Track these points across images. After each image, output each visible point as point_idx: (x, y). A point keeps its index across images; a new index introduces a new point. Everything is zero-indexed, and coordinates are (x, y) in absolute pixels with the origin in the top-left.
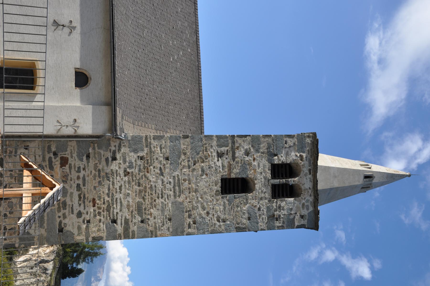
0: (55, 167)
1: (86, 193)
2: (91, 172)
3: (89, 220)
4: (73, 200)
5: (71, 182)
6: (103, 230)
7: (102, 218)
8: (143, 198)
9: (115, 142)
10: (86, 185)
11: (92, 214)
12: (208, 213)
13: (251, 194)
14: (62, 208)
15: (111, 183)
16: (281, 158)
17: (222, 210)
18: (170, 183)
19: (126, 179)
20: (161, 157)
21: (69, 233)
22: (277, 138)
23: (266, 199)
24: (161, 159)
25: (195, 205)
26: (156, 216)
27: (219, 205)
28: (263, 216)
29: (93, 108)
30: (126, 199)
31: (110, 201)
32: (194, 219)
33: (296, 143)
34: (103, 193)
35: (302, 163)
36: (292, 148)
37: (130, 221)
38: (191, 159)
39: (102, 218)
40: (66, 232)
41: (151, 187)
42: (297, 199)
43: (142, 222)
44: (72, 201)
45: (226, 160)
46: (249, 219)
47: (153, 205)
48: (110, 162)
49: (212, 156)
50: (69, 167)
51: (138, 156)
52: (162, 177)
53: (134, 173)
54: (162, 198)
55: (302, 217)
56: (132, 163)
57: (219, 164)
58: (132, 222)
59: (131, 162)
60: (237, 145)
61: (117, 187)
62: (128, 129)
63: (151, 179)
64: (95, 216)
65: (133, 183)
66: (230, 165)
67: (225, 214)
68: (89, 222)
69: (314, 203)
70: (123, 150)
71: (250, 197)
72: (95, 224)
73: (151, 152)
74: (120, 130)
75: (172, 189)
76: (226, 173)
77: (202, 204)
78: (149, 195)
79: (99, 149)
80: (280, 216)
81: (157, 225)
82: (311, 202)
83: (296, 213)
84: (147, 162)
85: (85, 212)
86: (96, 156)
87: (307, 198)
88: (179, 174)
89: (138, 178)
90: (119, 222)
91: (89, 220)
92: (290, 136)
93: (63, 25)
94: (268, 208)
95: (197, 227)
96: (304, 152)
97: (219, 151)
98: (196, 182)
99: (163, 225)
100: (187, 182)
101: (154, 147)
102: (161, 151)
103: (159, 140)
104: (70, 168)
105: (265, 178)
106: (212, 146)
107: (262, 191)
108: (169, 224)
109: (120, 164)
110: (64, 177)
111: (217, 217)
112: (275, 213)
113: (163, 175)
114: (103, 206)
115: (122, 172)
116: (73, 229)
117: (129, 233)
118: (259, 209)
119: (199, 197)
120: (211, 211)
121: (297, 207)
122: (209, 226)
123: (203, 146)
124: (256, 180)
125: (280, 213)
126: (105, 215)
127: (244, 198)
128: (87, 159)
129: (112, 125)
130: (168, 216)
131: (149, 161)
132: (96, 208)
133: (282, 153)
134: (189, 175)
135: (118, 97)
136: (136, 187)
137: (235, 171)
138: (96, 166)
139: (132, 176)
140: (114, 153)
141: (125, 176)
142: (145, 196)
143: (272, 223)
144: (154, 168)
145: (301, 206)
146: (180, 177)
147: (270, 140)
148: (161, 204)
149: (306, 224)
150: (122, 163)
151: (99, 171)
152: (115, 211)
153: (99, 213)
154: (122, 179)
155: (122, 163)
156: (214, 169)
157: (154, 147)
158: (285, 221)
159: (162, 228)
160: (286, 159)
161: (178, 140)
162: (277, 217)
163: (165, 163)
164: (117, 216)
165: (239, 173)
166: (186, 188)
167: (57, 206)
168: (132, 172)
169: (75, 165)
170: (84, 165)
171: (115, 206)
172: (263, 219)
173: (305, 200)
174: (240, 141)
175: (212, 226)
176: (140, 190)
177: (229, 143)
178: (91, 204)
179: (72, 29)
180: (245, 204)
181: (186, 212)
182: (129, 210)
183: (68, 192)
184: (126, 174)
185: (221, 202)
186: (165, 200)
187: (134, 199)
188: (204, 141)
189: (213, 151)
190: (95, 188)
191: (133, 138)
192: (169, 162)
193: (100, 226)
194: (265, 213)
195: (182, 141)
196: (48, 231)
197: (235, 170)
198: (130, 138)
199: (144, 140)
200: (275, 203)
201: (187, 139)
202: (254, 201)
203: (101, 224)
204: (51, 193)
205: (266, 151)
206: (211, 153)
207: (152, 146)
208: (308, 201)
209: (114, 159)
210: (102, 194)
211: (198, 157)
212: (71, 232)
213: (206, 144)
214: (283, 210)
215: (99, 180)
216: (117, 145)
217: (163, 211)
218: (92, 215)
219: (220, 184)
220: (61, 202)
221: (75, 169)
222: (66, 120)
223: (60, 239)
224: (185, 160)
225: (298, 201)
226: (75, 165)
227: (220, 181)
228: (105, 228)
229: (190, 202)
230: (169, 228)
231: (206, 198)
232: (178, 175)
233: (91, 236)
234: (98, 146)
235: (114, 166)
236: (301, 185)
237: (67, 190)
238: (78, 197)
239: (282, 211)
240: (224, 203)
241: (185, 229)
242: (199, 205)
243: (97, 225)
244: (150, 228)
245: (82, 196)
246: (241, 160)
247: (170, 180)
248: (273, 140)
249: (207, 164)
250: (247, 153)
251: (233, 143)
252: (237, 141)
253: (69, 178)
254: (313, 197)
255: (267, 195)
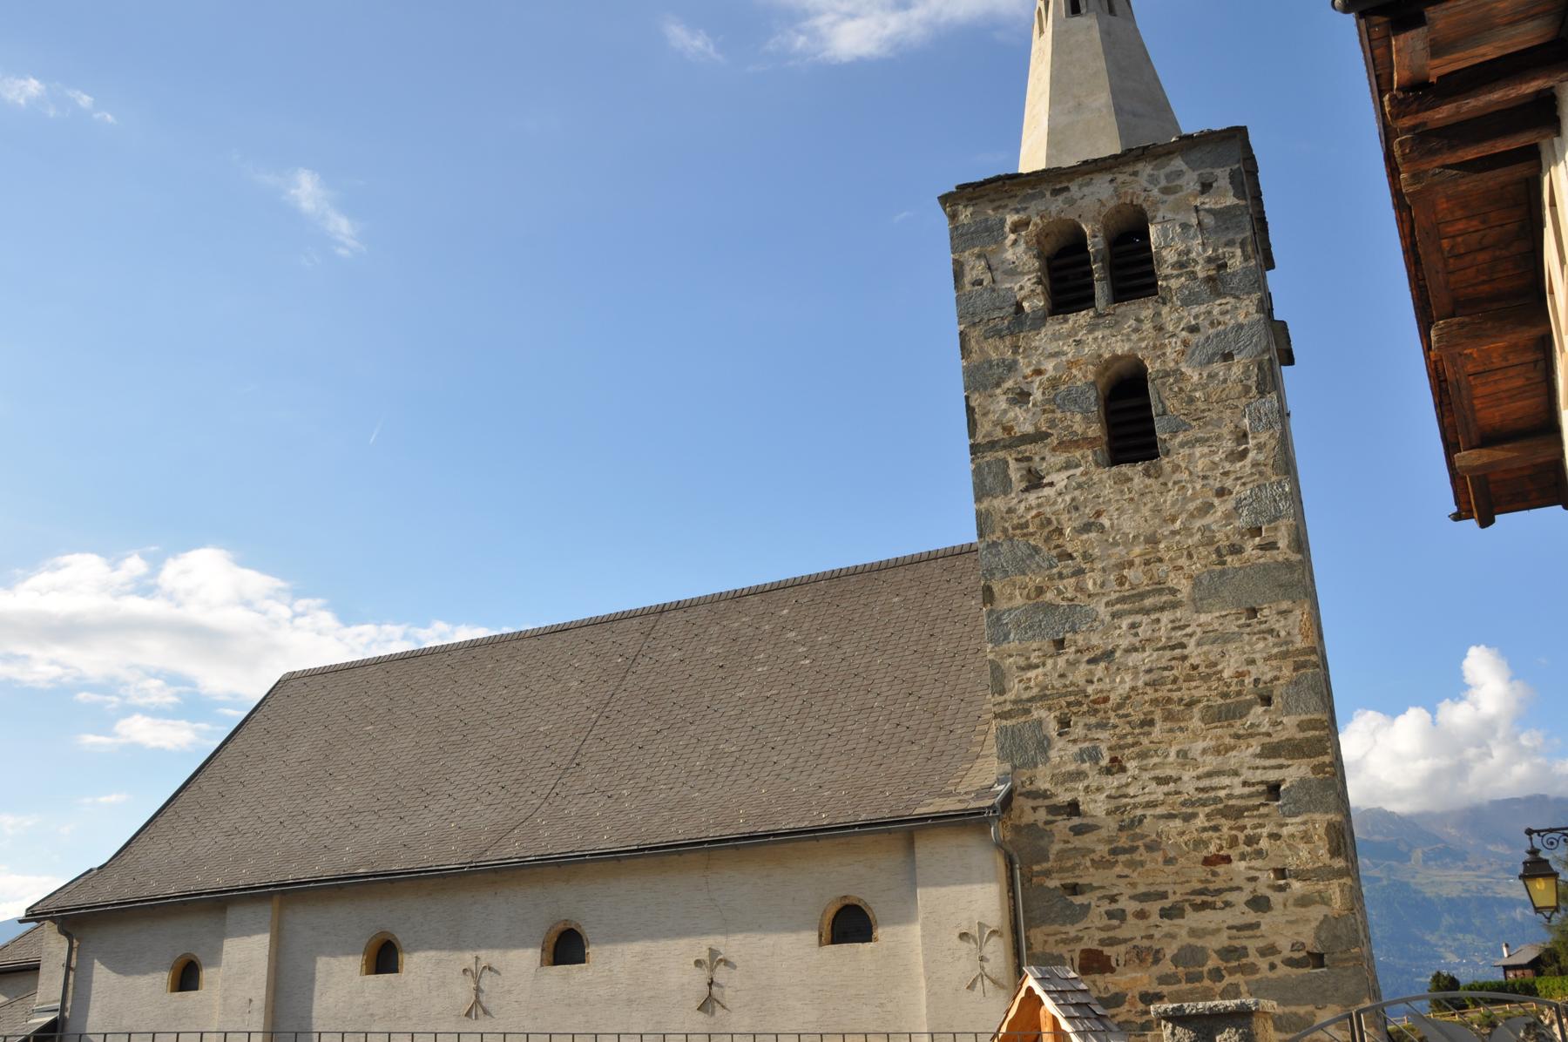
0: (1113, 989)
1: (1188, 888)
2: (1120, 876)
3: (1275, 870)
4: (1213, 926)
5: (1157, 935)
6: (1304, 823)
7: (1265, 831)
8: (1191, 704)
9: (1022, 811)
10: (1162, 889)
11: (1253, 863)
12: (1222, 492)
13: (1147, 363)
14: (1244, 961)
15: (1149, 812)
16: (1028, 289)
17: (1206, 450)
18: (1133, 626)
19: (1132, 765)
20: (1055, 664)
21: (1323, 936)
22: (967, 314)
23: (1158, 314)
24: (1061, 661)
25: (1198, 536)
26: (1246, 659)
27: (1191, 459)
28: (1216, 312)
29: (925, 885)
30: (1202, 761)
31: (1207, 810)
32: (1243, 535)
33: (976, 250)
34: (1182, 833)
35: (1036, 219)
36: (994, 262)
37: (1267, 740)
38: (1055, 571)
39: (1265, 831)
40: (1321, 942)
41: (1152, 684)
42: (1149, 215)
43: (1267, 701)
44: (1218, 930)
45: (1049, 460)
46: (1227, 357)
47: (1210, 672)
48: (1085, 821)
49: (1039, 506)
50: (1111, 945)
51: (1060, 735)
52: (1117, 654)
53: (1114, 741)
54: (1183, 646)
55: (1206, 187)
56: (1082, 751)
57: (1060, 479)
58: (1269, 735)
59: (1081, 756)
60: (999, 434)
61: (1159, 792)
62: (984, 776)
63: (1127, 686)
64: (1259, 854)
65: (1145, 741)
66: (1063, 445)
67: (1219, 438)
68: (1281, 873)
69: (1157, 157)
70: (1044, 784)
71: (1157, 365)
72: (1288, 852)
73: (1043, 697)
74: (982, 798)
75: (1153, 617)
76: (1089, 452)
77: (1192, 516)
78: (1180, 689)
79: (1047, 859)
80: (1209, 260)
81: (1275, 650)
82: (1156, 168)
83: (1197, 209)
84: (1075, 707)
85: (1249, 887)
86: (1069, 864)
87: (1145, 184)
88: (1105, 600)
89: (1128, 729)
90: (1273, 776)
91: (1275, 870)
92: (958, 275)
93: (710, 985)
94: (1187, 302)
95: (1270, 522)
96: (1003, 221)
97: (1023, 485)
98: (1125, 544)
99: (1271, 631)
100: (1125, 572)
101: (1026, 689)
102: (1037, 667)
103: (1003, 675)
104: (1112, 942)
105: (1092, 328)
106: (1010, 511)
107: (1136, 330)
108: (1266, 612)
109: (1087, 788)
110: (1142, 961)
111: (1232, 462)
112: (1201, 275)
113: (1113, 652)
114: (1225, 829)
115: (1113, 782)
116: (1308, 920)
117: (1307, 739)
118: (1193, 329)
119: (1172, 528)
120: (1211, 482)
121: (1177, 208)
122: (1262, 481)
123: (1011, 539)
124: (1100, 356)
125: (1201, 261)
126: (1256, 821)
127: (1164, 384)
128: (1082, 893)
129: (965, 824)
130: (1243, 621)
131: (1072, 698)
132: (1234, 854)
133: (1011, 289)
134: (1104, 570)
135: (885, 814)
136: (1157, 732)
137: (1078, 427)
138: (1100, 864)
139: (1121, 747)
140: (1054, 810)
141: (1123, 770)
142: (1181, 700)
143: (1236, 280)
144: (1090, 682)
145: (1172, 197)
146: (1114, 596)
147: (975, 333)
148: (1205, 648)
149: (1228, 169)
150: (1086, 783)
151: (1114, 852)
152: (1238, 791)
153: (1250, 841)
154: (1135, 778)
155: (1086, 783)
156: (1077, 493)
157: (1026, 689)
158: (1224, 240)
159: (1283, 634)
160: (1029, 272)
161: (999, 619)
162: (1213, 266)
163: (1073, 649)
164: (1253, 784)
165: (1085, 412)
166: (1145, 573)
167: (1238, 975)
168: (1110, 749)
169: (1101, 929)
170: (1099, 899)
171: (1222, 793)
172: (1224, 313)
173: (1150, 187)
174: (985, 427)
175: (1261, 474)
176: (1165, 719)
177: (997, 458)
178: (1221, 869)
179: (715, 959)
180: (1179, 375)
181: (1224, 563)
182: (1233, 748)
183: (1190, 946)
184: (1116, 766)
185: (1179, 457)
186: (1191, 635)
187: (1196, 736)
188: (997, 536)
189: (1022, 506)
190: (1169, 861)
191: (1004, 756)
192: (1068, 635)
193: (1292, 836)
194: (1203, 308)
195: (1002, 605)
196: (1321, 1000)
197: (1076, 427)
198: (1007, 767)
199: (1008, 723)
200: (1171, 280)
201: (995, 589)
202: (1169, 350)
203: (1285, 831)
204: (1049, 1006)
205: (1008, 340)
206: (1029, 509)
207: (1025, 696)
208: (1153, 180)
209: (1073, 808)
210: (1186, 838)
211: (1045, 549)
212: (1319, 928)
213: (1005, 530)
214: (1188, 252)
215: (1142, 849)
216: (1031, 803)
217: (1225, 639)
218: (1258, 863)
219: (1125, 468)
220: (1222, 965)
221: (1115, 928)
222: (963, 963)
223: (1346, 960)
224: (1058, 589)
225: (1158, 210)
226: (1101, 929)
227: (1114, 469)
228: (1298, 819)
229: (1190, 556)
230: (1280, 613)
231: (1173, 504)
232: (1107, 604)
233: (1328, 861)
234: (1038, 862)
235: (1096, 808)
236: (1104, 211)
237: (1181, 949)
238: (1203, 913)
239: (1193, 255)
240: (1182, 445)
241: (1280, 559)
242: (1198, 523)
243: (1290, 846)
244: (1287, 672)
245: (1199, 899)
246: (1044, 411)
247: (1124, 627)
248: (974, 324)
249: (1065, 517)
250: (1021, 397)
251: (992, 445)
252: (989, 434)
253: (1146, 943)
254: (1140, 166)
255: (1147, 313)
